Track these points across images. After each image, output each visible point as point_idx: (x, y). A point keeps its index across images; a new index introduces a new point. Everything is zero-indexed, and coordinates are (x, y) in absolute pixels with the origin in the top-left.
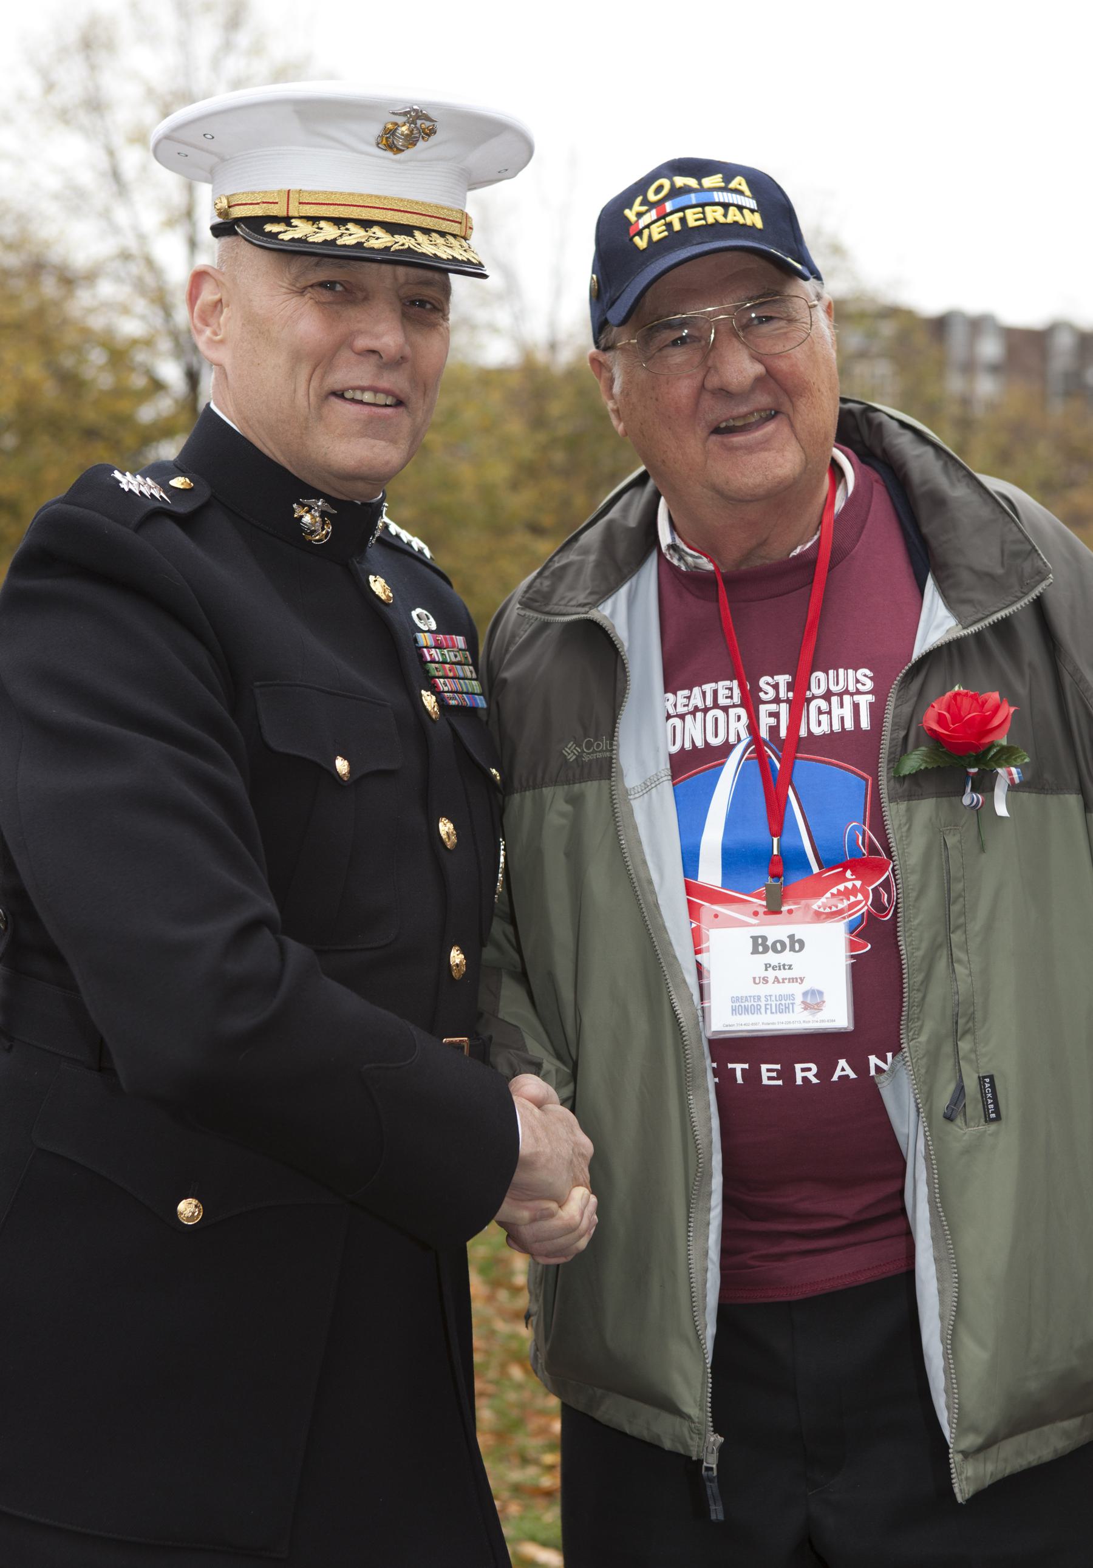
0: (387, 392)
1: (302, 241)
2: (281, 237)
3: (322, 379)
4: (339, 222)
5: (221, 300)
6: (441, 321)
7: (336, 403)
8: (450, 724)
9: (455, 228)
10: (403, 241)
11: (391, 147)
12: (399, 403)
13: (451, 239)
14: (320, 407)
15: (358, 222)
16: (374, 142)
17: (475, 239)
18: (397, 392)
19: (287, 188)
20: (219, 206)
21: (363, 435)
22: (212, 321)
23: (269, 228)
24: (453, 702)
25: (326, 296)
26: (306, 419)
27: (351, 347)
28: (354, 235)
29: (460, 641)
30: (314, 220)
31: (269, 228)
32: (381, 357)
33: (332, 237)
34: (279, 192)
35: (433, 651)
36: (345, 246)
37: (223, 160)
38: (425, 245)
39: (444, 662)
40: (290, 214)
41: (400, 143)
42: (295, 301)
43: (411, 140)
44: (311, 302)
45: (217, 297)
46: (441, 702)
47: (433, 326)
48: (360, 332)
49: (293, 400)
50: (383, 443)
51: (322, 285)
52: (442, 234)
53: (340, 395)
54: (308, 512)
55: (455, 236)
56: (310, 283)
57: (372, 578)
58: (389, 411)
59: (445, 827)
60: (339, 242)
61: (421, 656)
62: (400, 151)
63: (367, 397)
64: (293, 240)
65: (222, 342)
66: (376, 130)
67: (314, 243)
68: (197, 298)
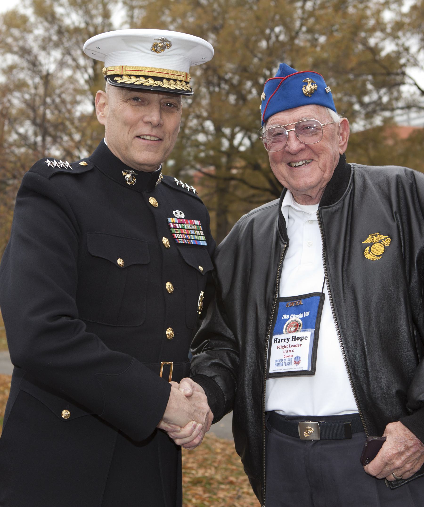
0: (155, 136)
2: (118, 82)
11: (156, 51)
12: (160, 140)
18: (158, 136)
19: (122, 65)
25: (135, 103)
27: (142, 120)
30: (130, 76)
31: (116, 79)
36: (137, 85)
37: (106, 56)
40: (123, 74)
41: (159, 49)
48: (145, 115)
53: (139, 137)
62: (159, 52)
63: (148, 138)
64: (121, 83)
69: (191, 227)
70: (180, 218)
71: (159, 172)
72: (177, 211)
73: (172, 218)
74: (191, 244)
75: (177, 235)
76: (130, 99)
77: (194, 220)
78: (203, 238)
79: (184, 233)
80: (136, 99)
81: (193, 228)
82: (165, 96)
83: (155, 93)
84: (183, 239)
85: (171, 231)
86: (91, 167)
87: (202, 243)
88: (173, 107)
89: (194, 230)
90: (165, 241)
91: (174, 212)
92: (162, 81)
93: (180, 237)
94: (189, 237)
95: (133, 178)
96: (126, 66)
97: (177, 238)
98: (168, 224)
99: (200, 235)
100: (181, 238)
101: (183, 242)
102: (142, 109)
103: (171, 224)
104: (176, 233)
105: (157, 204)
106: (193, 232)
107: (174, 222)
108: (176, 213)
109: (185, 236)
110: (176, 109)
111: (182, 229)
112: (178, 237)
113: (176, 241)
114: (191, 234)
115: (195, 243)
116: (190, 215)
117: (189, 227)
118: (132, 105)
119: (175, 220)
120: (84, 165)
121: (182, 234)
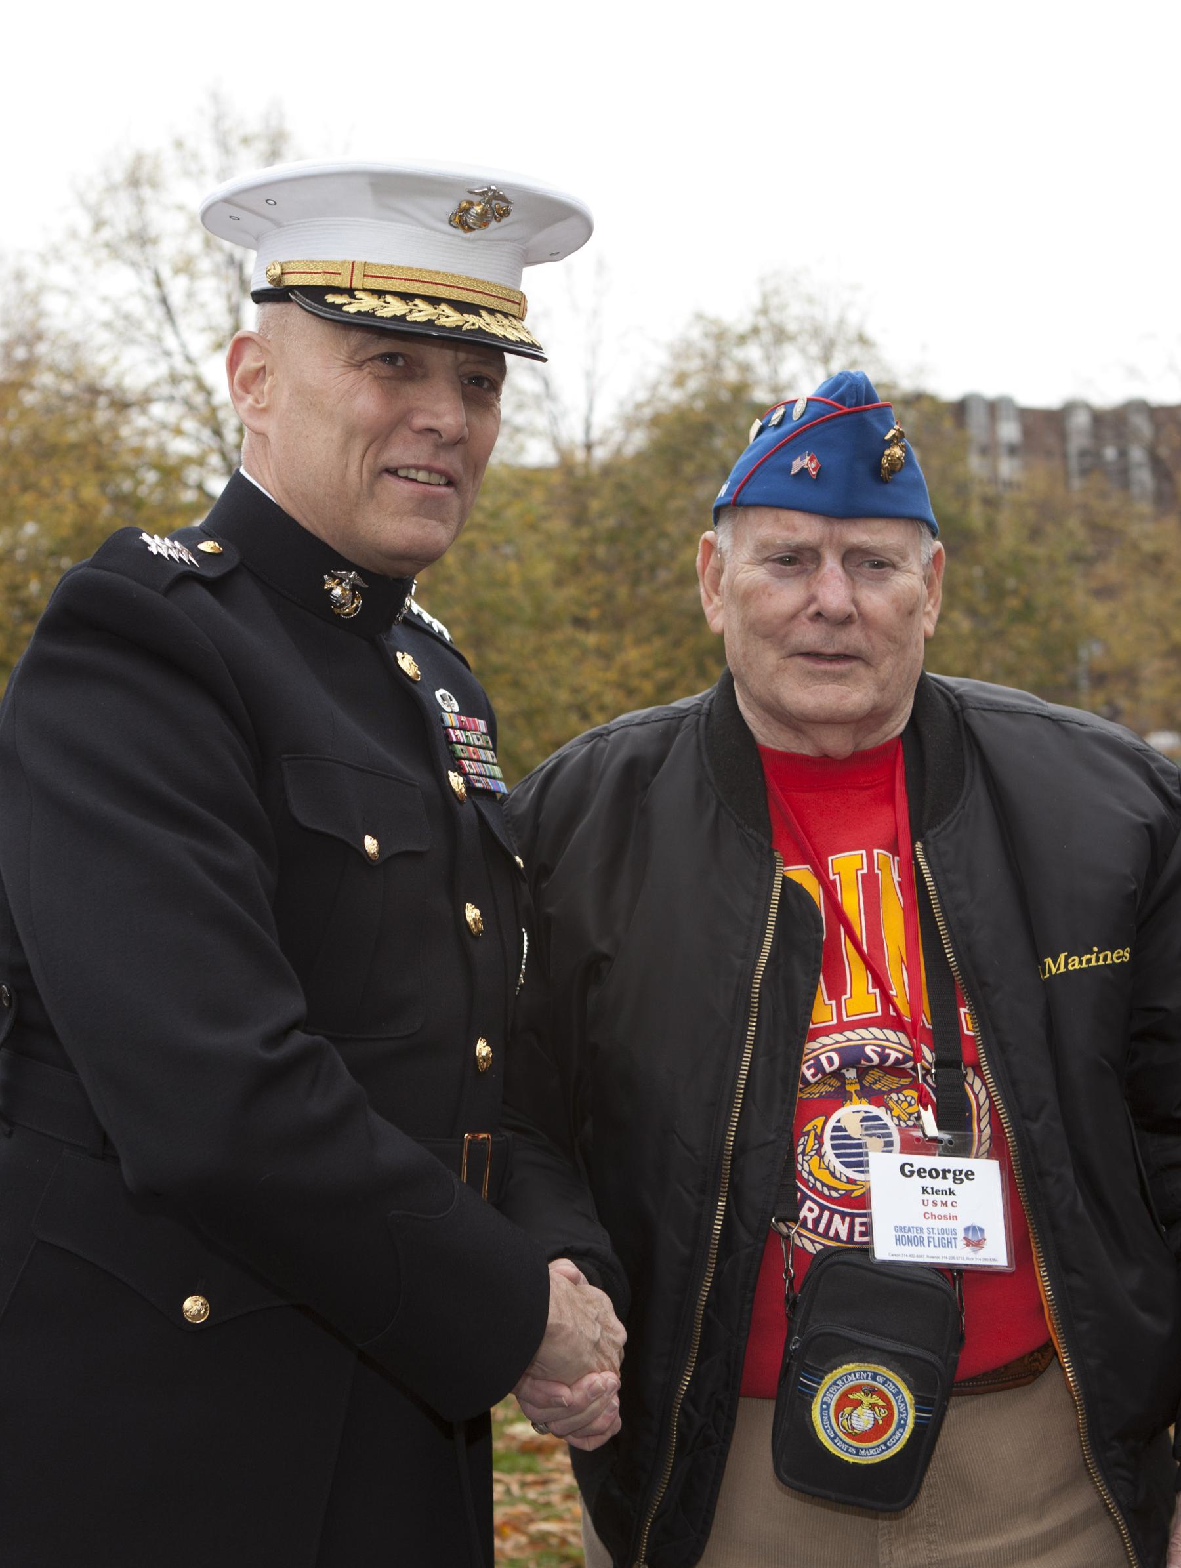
0: (441, 473)
1: (370, 314)
2: (346, 308)
3: (377, 455)
4: (406, 297)
5: (264, 367)
7: (388, 480)
8: (476, 807)
10: (472, 321)
12: (450, 483)
14: (371, 485)
15: (427, 299)
17: (527, 323)
18: (452, 473)
20: (272, 272)
21: (415, 513)
22: (253, 388)
23: (330, 298)
24: (479, 785)
25: (385, 369)
26: (358, 496)
27: (409, 425)
28: (422, 313)
29: (482, 725)
30: (380, 293)
31: (330, 298)
32: (440, 436)
33: (402, 313)
34: (343, 263)
35: (458, 732)
36: (415, 322)
39: (468, 745)
41: (470, 221)
42: (352, 375)
43: (484, 220)
46: (468, 783)
49: (343, 477)
50: (434, 523)
51: (383, 357)
52: (506, 315)
53: (392, 472)
54: (338, 584)
56: (370, 356)
57: (399, 655)
58: (443, 490)
59: (472, 913)
61: (448, 736)
62: (471, 229)
64: (359, 313)
66: (449, 207)
67: (382, 317)
68: (237, 364)
82: (472, 357)
95: (354, 596)
118: (377, 378)
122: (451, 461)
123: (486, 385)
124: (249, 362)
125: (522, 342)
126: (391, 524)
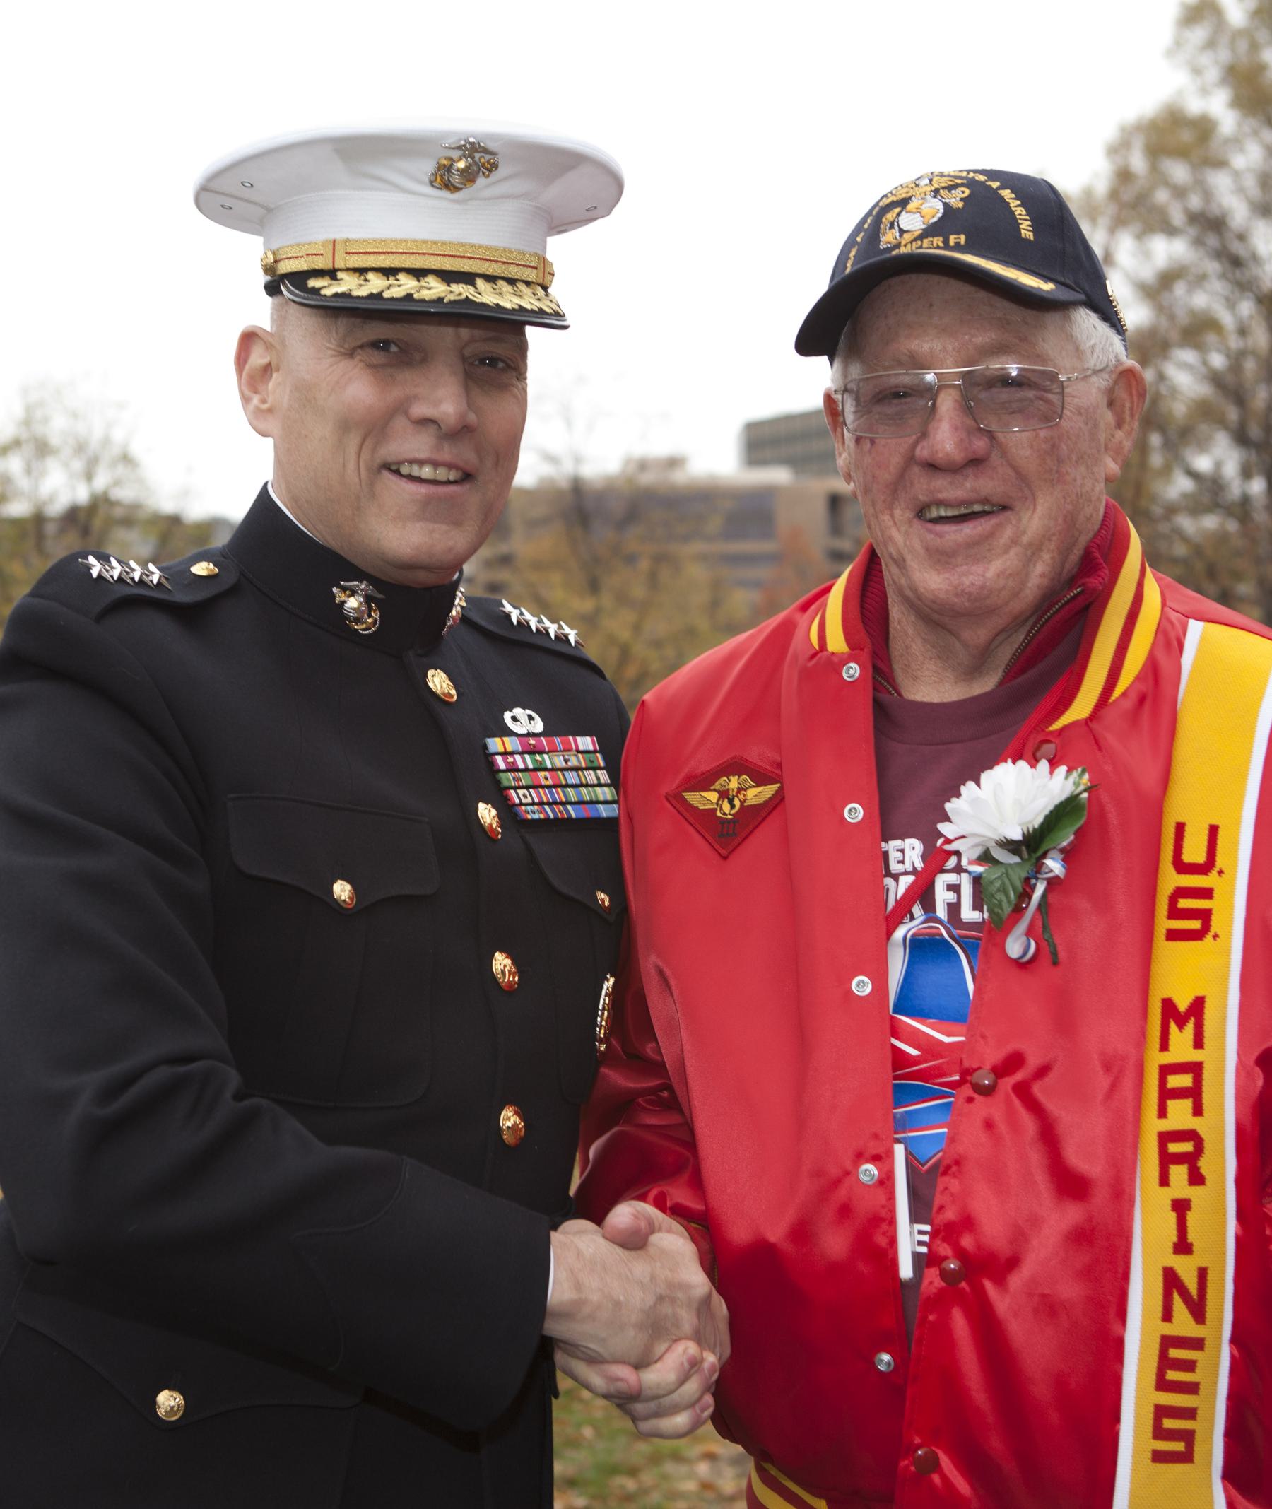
1: (346, 296)
2: (323, 292)
3: (374, 450)
5: (269, 364)
6: (515, 381)
9: (530, 275)
10: (460, 291)
11: (448, 186)
12: (467, 477)
13: (522, 287)
16: (427, 180)
18: (461, 464)
19: (332, 237)
23: (312, 283)
25: (378, 357)
27: (406, 413)
28: (405, 285)
30: (361, 271)
31: (312, 283)
34: (324, 243)
36: (392, 299)
38: (486, 295)
41: (456, 179)
42: (345, 365)
43: (469, 176)
44: (361, 365)
45: (265, 361)
47: (504, 387)
51: (375, 345)
52: (511, 281)
53: (392, 468)
55: (528, 283)
56: (359, 343)
60: (386, 295)
62: (457, 189)
63: (427, 472)
64: (336, 295)
65: (270, 410)
66: (428, 167)
68: (245, 362)
69: (566, 761)
70: (529, 735)
71: (455, 586)
72: (518, 711)
73: (501, 736)
74: (570, 819)
75: (521, 792)
76: (361, 347)
77: (574, 735)
78: (606, 793)
79: (544, 782)
80: (379, 345)
81: (573, 762)
82: (477, 333)
83: (448, 324)
84: (541, 803)
85: (498, 782)
86: (232, 579)
87: (604, 811)
88: (503, 370)
89: (576, 769)
90: (487, 813)
91: (507, 716)
92: (473, 285)
93: (529, 800)
94: (559, 795)
95: (370, 608)
96: (347, 241)
97: (521, 804)
98: (489, 758)
99: (600, 785)
100: (533, 804)
101: (542, 816)
102: (406, 375)
103: (499, 759)
104: (515, 788)
105: (453, 692)
106: (572, 778)
107: (509, 749)
108: (514, 719)
109: (545, 795)
110: (514, 374)
111: (535, 770)
112: (524, 801)
113: (516, 815)
114: (567, 786)
115: (583, 815)
116: (561, 723)
117: (559, 762)
118: (370, 366)
119: (511, 744)
120: (204, 573)
121: (536, 787)
122: (465, 454)
123: (501, 365)
124: (258, 358)
125: (541, 311)
126: (398, 530)
